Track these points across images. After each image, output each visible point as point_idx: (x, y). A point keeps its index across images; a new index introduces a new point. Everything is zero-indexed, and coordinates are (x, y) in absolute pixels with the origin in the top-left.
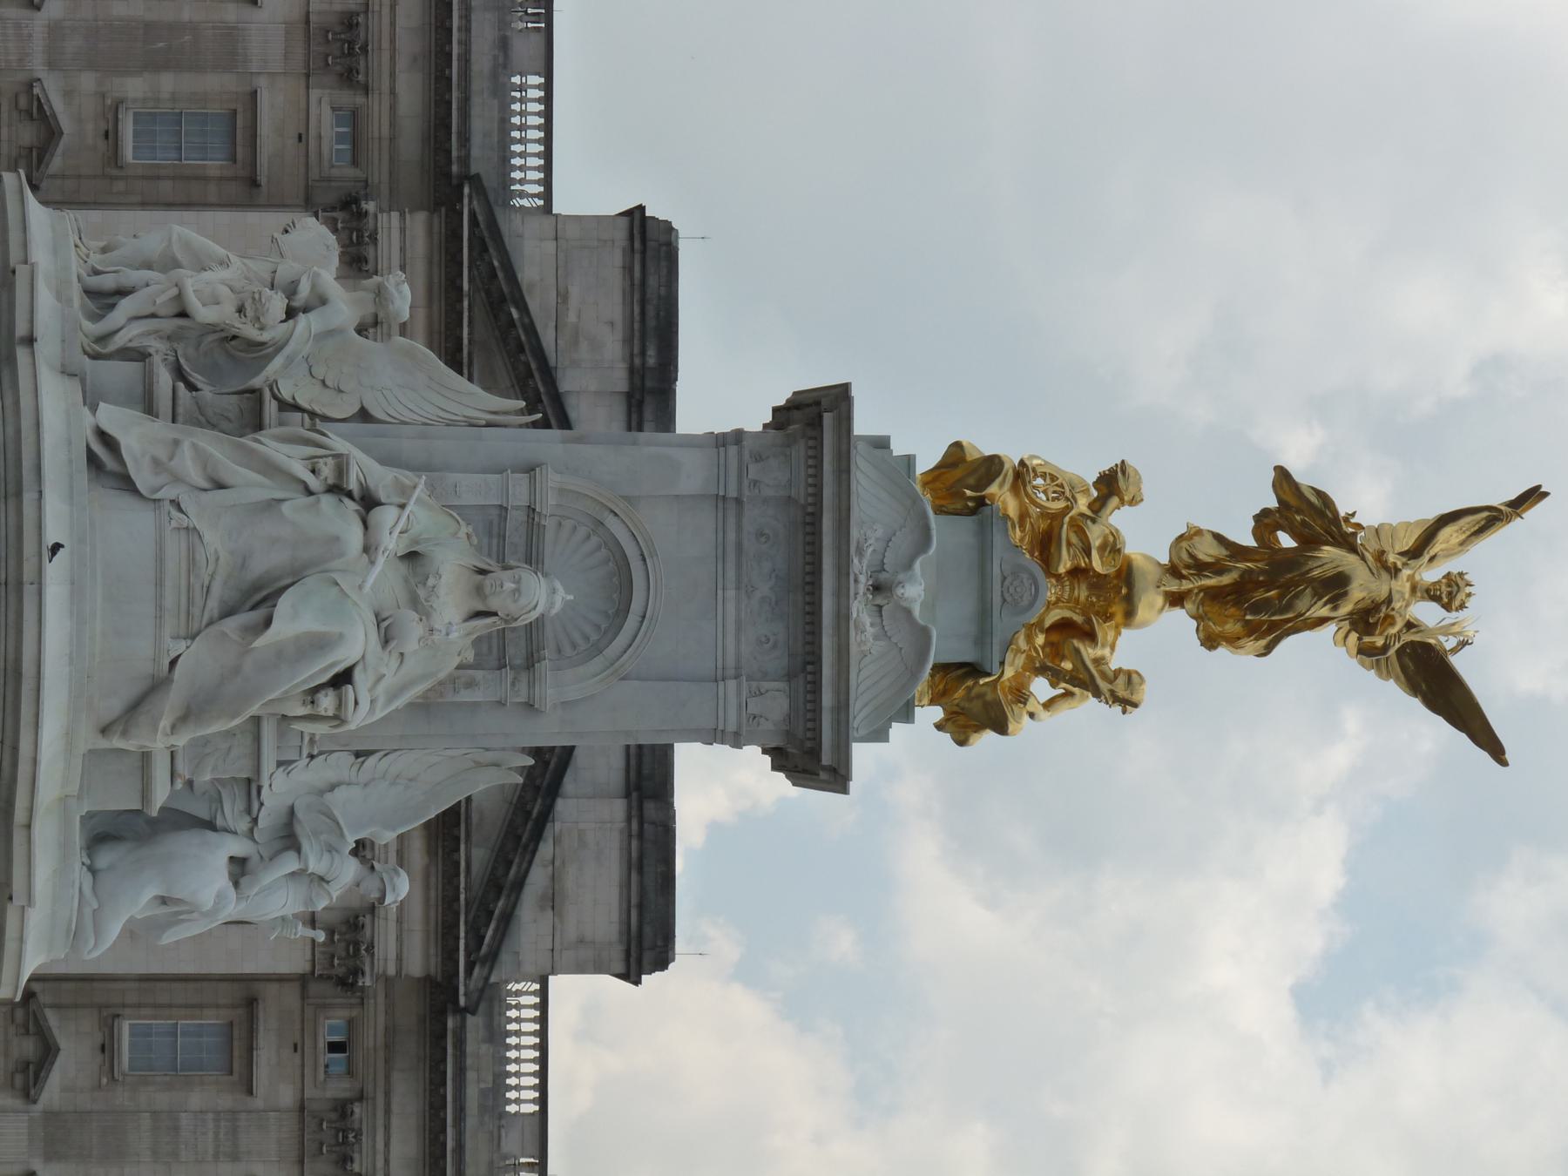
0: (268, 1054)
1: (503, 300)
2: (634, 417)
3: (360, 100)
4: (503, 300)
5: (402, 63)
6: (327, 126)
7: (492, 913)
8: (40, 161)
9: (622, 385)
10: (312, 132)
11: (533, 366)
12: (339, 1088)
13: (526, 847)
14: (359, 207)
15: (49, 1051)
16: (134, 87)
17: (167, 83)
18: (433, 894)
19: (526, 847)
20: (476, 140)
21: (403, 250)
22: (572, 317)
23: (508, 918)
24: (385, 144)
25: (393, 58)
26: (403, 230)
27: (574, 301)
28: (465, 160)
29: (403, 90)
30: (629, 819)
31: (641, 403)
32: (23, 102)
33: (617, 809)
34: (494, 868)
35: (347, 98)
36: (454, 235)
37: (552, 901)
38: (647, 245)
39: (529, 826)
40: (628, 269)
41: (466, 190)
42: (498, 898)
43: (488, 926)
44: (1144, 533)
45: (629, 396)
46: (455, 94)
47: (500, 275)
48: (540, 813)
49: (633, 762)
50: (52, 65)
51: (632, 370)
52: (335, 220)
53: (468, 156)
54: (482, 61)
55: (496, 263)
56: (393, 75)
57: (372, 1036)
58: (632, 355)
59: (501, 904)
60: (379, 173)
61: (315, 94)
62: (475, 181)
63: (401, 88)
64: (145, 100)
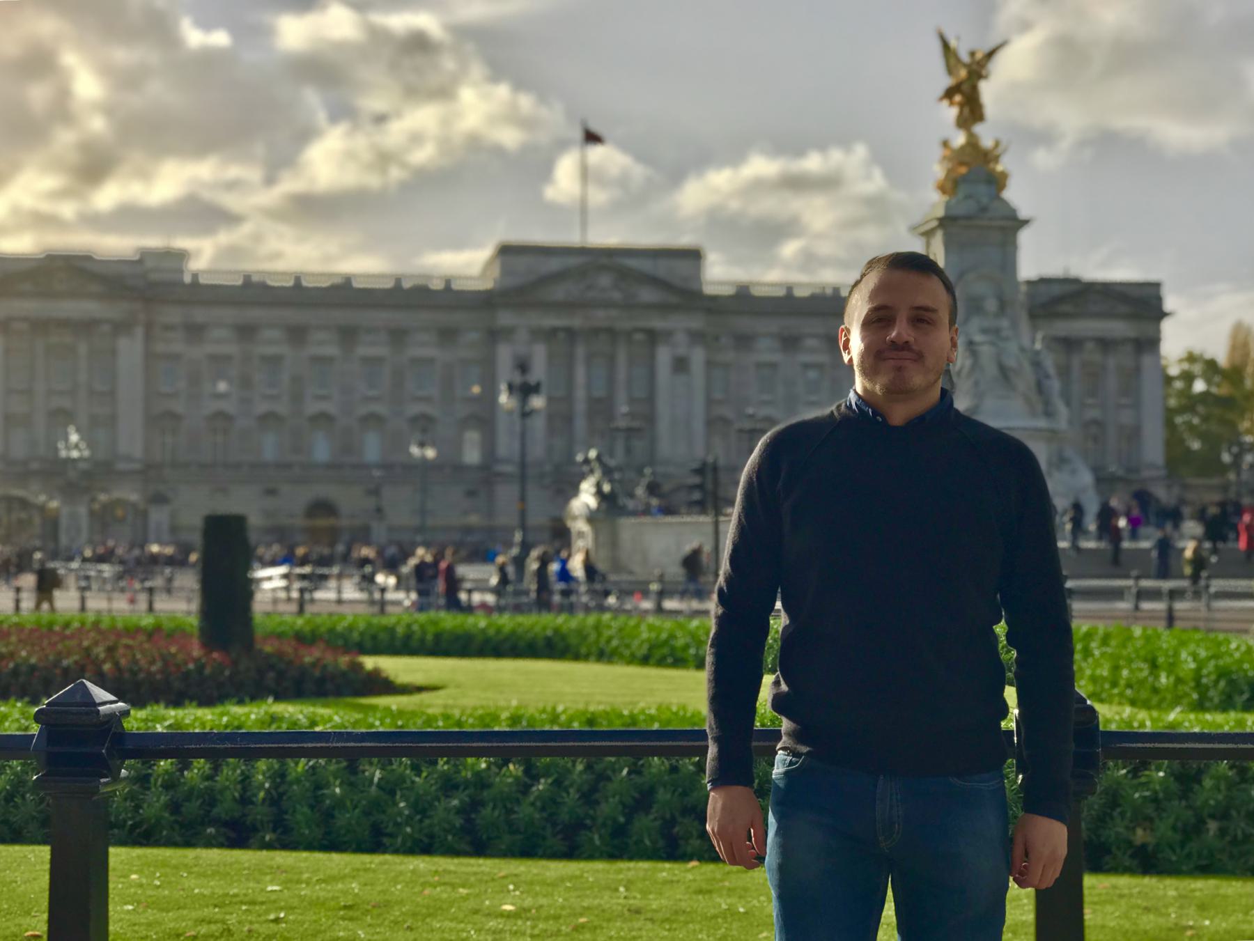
38: (506, 251)
44: (959, 139)
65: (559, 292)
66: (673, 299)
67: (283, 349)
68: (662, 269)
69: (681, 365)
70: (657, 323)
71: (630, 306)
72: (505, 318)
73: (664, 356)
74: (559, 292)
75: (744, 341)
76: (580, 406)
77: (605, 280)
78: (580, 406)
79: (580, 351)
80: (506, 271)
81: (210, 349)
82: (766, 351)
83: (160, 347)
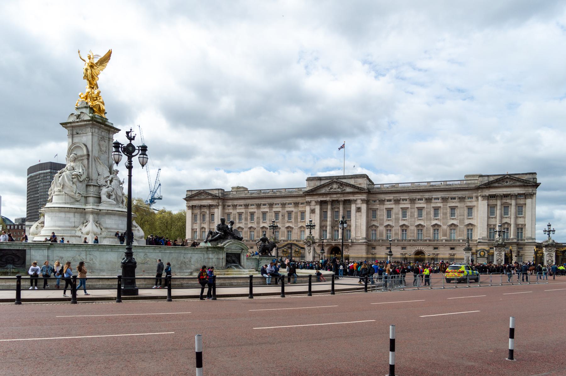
0: (375, 207)
12: (377, 201)
15: (374, 225)
16: (299, 220)
29: (299, 200)
33: (353, 180)
37: (360, 184)
38: (309, 179)
57: (373, 199)
65: (323, 191)
66: (356, 190)
67: (255, 210)
68: (352, 182)
69: (359, 210)
70: (351, 198)
71: (343, 193)
72: (308, 199)
73: (353, 207)
74: (323, 191)
75: (382, 202)
76: (329, 223)
77: (335, 186)
80: (309, 185)
81: (238, 211)
82: (388, 205)
83: (227, 211)
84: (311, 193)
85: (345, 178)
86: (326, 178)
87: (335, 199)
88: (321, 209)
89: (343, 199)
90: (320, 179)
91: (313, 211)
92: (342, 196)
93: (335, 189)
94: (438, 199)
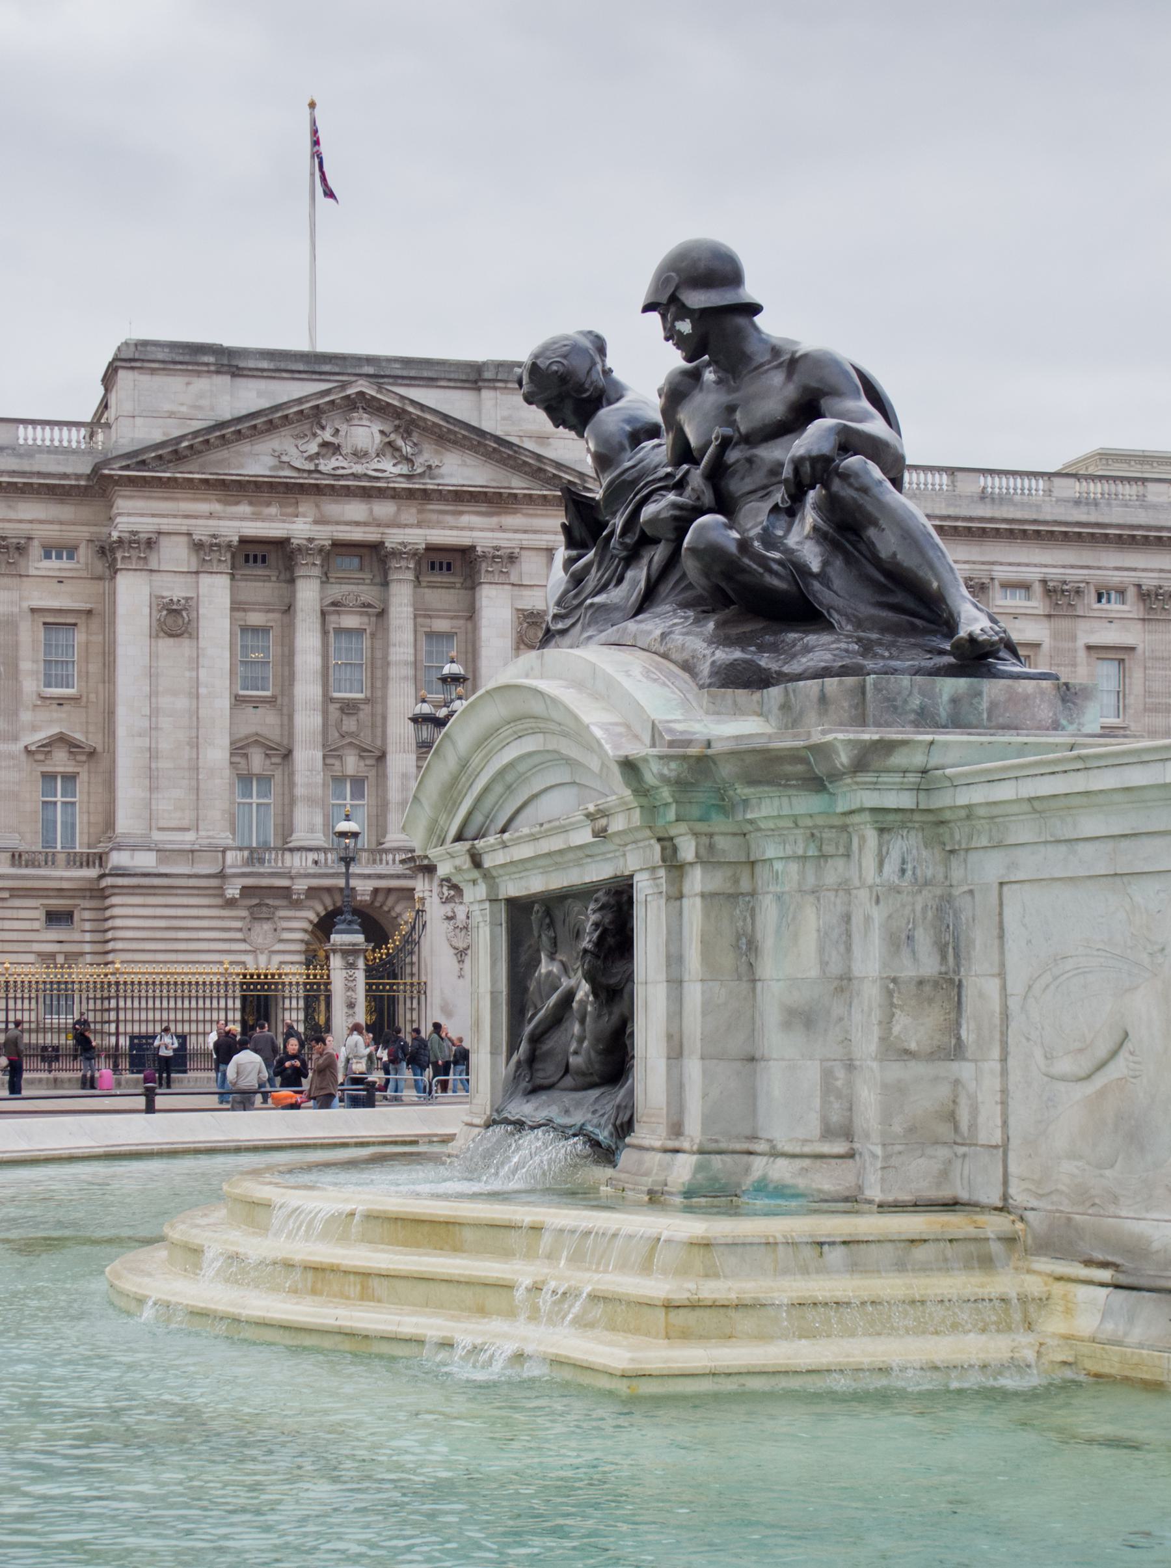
1: (176, 452)
2: (245, 373)
3: (36, 543)
4: (176, 452)
5: (12, 515)
6: (53, 565)
7: (554, 475)
8: (79, 747)
9: (227, 378)
10: (57, 574)
11: (218, 434)
13: (515, 452)
14: (115, 542)
17: (25, 665)
18: (539, 512)
19: (515, 452)
20: (61, 469)
21: (142, 515)
22: (184, 409)
23: (559, 465)
24: (64, 527)
25: (9, 521)
26: (129, 515)
27: (174, 408)
28: (78, 477)
30: (495, 388)
31: (237, 367)
32: (40, 757)
34: (525, 473)
35: (35, 550)
36: (132, 481)
39: (503, 449)
40: (153, 371)
41: (106, 472)
42: (545, 471)
43: (560, 477)
45: (234, 375)
46: (35, 480)
47: (160, 452)
48: (495, 442)
49: (459, 385)
50: (16, 739)
51: (218, 372)
52: (124, 558)
53: (76, 475)
54: (11, 463)
55: (153, 455)
56: (20, 521)
58: (208, 372)
59: (548, 468)
60: (81, 533)
61: (32, 572)
62: (96, 469)
63: (29, 517)
64: (38, 680)
65: (256, 461)
66: (518, 484)
72: (133, 514)
74: (256, 461)
76: (308, 721)
77: (365, 433)
78: (308, 721)
79: (308, 593)
84: (164, 467)
85: (430, 382)
86: (282, 364)
87: (357, 535)
88: (237, 607)
89: (417, 536)
90: (228, 362)
91: (175, 620)
92: (410, 513)
93: (359, 455)
94: (1026, 587)
